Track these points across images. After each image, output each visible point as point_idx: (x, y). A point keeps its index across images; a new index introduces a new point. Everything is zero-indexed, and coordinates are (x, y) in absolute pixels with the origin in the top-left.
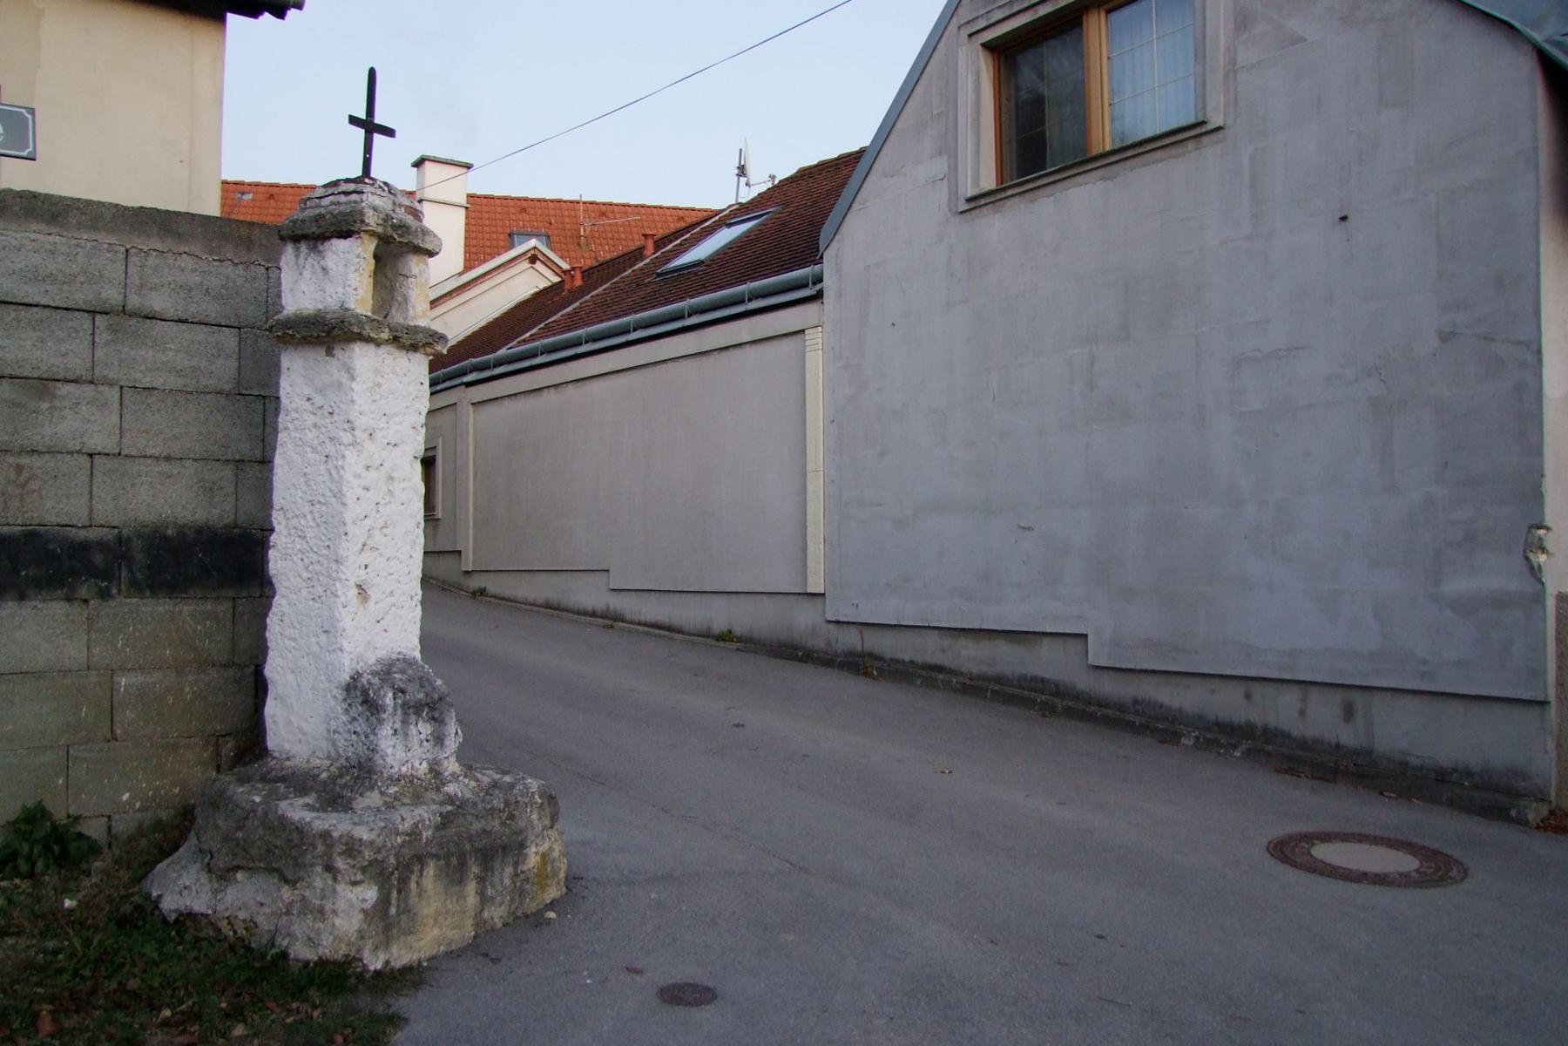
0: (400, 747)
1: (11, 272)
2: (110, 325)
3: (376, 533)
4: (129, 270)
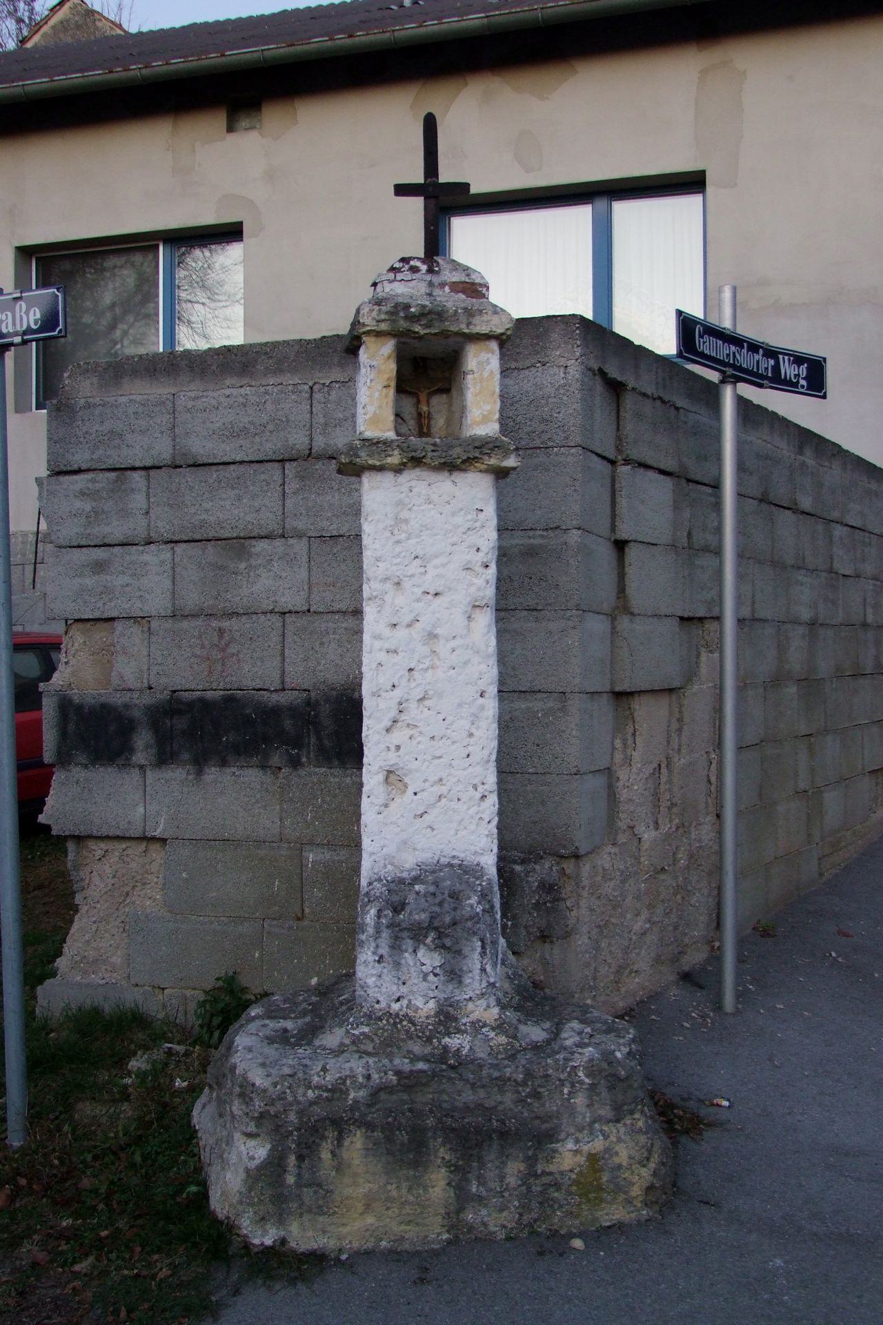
0: (387, 977)
1: (211, 433)
2: (298, 472)
3: (412, 706)
4: (314, 409)
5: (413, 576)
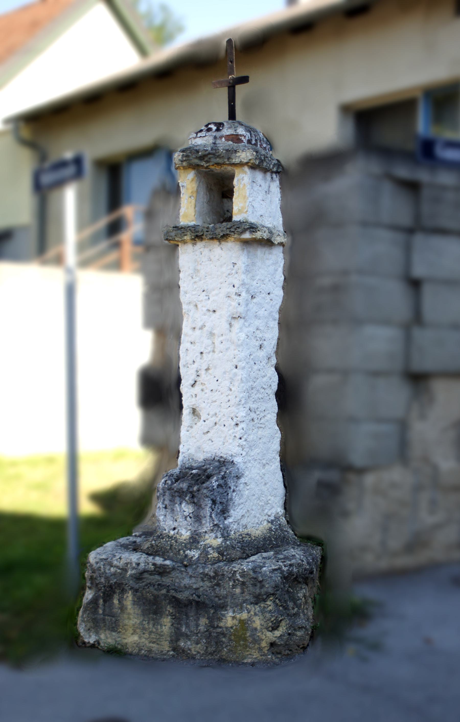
0: (169, 517)
5: (202, 301)
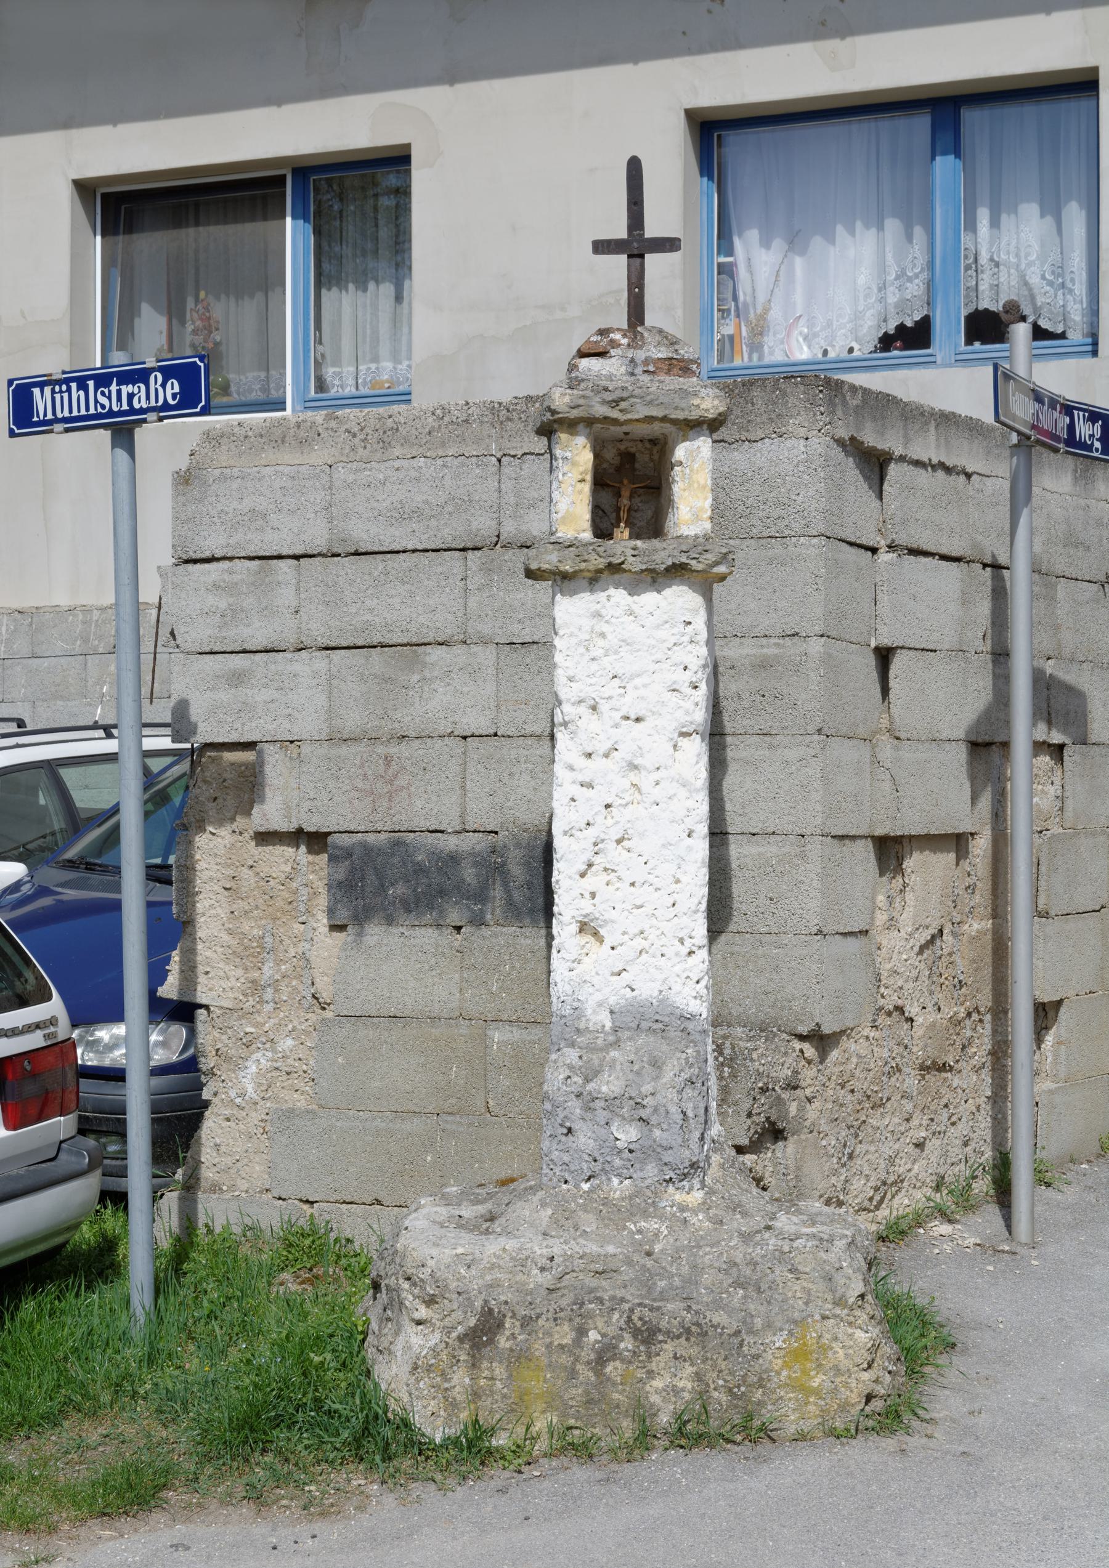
4: (503, 486)
5: (610, 698)
